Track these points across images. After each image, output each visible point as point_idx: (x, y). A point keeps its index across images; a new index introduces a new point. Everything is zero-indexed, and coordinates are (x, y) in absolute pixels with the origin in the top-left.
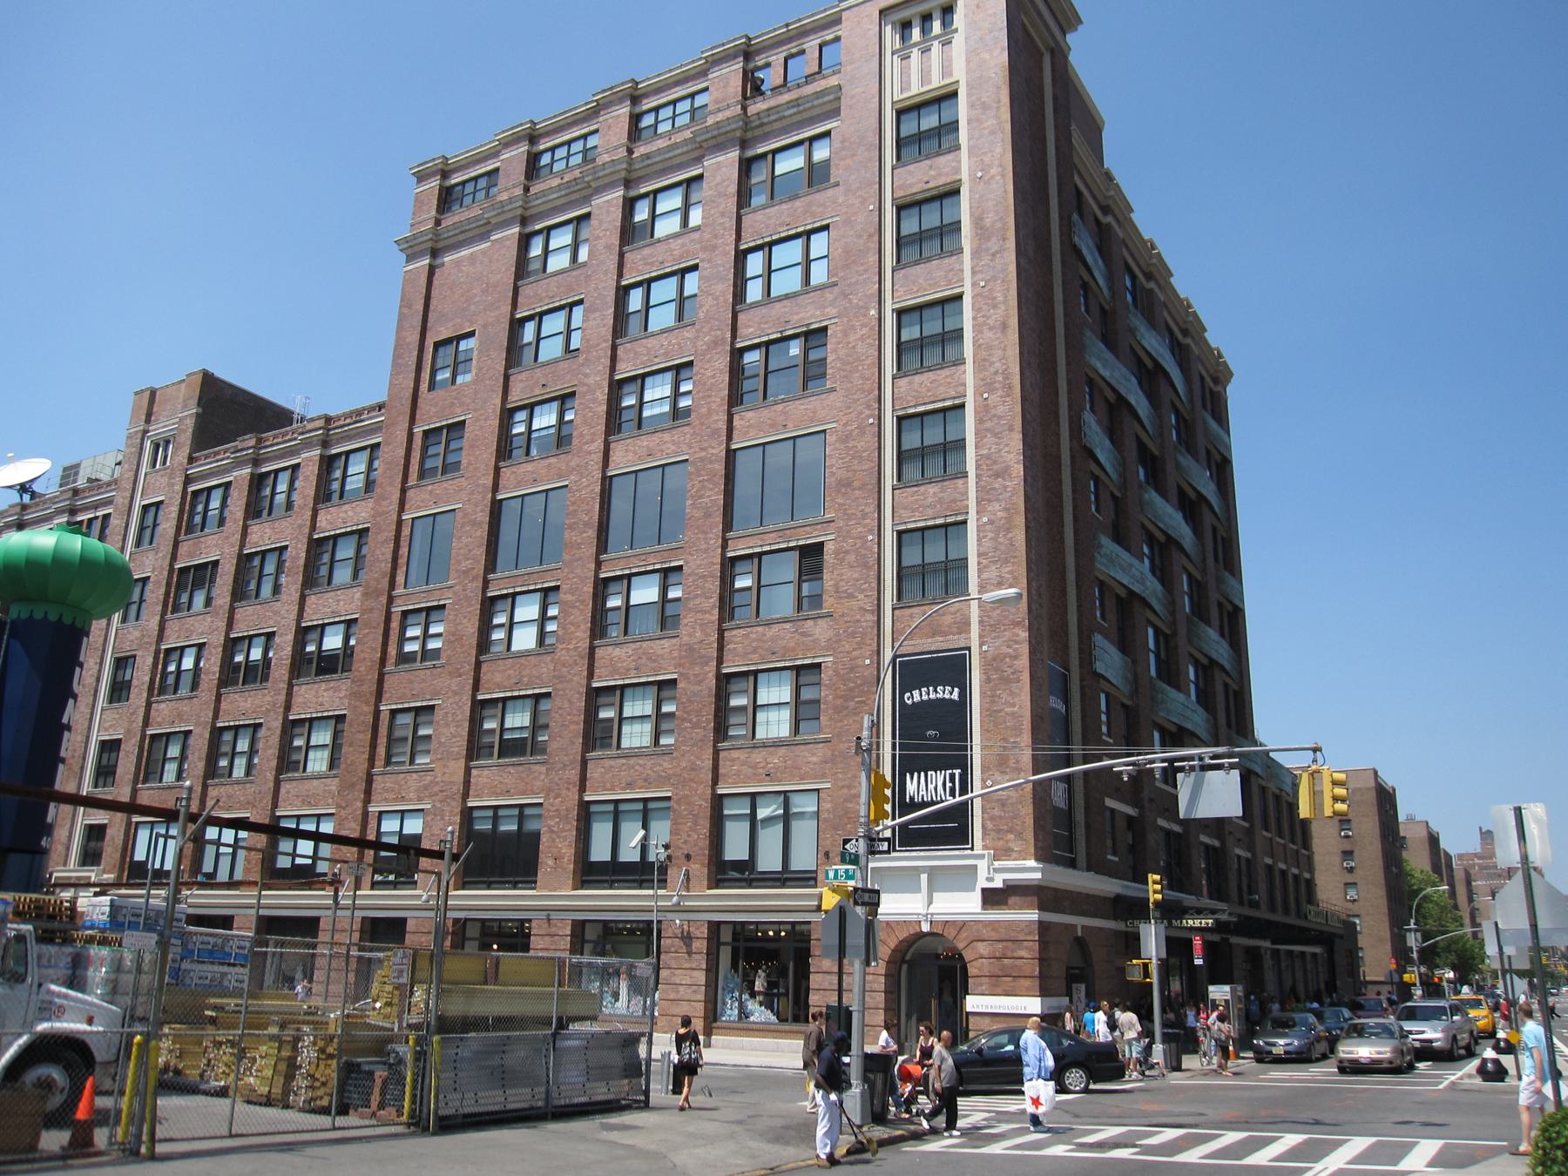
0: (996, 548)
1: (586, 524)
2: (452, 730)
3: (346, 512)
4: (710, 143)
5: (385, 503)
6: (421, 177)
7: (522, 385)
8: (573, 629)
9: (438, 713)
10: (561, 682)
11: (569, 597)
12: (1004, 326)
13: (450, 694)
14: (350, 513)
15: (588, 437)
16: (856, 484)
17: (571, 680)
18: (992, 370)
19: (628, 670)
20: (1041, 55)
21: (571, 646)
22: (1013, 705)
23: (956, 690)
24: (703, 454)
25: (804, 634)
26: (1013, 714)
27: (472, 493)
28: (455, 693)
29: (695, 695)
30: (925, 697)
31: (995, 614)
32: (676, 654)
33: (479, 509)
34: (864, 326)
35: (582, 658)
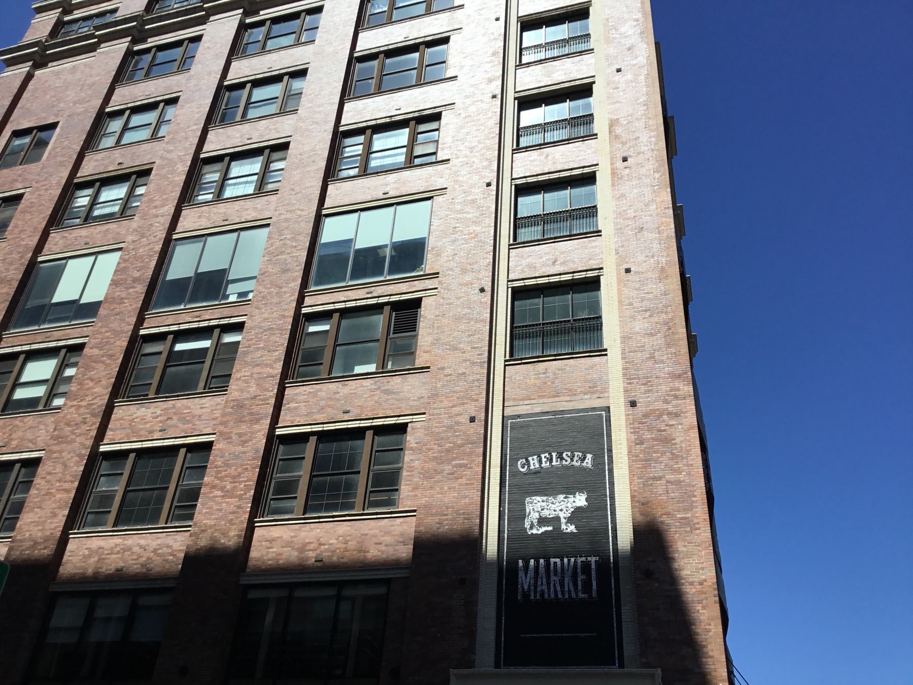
1: (135, 280)
7: (95, 164)
8: (91, 384)
10: (59, 443)
11: (96, 351)
15: (157, 203)
17: (73, 441)
22: (679, 471)
23: (589, 456)
25: (387, 392)
26: (678, 482)
27: (11, 253)
29: (237, 457)
32: (217, 414)
33: (12, 268)
35: (94, 415)
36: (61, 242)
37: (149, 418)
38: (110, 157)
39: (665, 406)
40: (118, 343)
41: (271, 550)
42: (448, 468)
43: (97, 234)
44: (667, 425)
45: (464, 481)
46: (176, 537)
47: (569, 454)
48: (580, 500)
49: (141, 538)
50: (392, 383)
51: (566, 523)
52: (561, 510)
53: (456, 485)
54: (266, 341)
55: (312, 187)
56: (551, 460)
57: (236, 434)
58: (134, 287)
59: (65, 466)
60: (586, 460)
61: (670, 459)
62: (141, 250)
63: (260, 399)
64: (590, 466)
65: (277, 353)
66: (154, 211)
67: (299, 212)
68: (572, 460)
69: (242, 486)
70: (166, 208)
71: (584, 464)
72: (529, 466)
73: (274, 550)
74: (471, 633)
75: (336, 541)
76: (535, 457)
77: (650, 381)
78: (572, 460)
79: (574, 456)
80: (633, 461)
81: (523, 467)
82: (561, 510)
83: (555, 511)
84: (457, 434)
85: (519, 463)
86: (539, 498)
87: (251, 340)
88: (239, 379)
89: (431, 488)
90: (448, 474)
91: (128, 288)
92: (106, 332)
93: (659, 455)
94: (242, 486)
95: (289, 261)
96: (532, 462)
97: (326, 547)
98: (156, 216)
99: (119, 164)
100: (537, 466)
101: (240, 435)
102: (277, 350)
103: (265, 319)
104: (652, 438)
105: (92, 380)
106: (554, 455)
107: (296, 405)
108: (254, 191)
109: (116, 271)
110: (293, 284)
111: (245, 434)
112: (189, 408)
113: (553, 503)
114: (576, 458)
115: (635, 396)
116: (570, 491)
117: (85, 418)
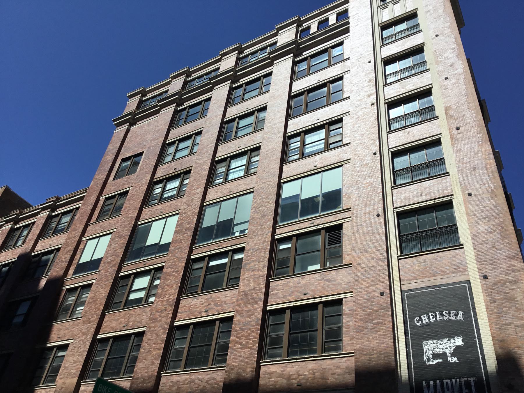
1: (187, 229)
2: (75, 358)
3: (53, 241)
5: (75, 232)
7: (163, 170)
8: (168, 288)
9: (70, 348)
10: (153, 322)
11: (169, 270)
13: (81, 335)
14: (55, 241)
15: (195, 187)
17: (161, 321)
19: (200, 313)
21: (165, 299)
23: (461, 313)
27: (124, 222)
28: (84, 334)
29: (247, 324)
32: (235, 300)
33: (125, 229)
35: (170, 305)
36: (148, 213)
37: (199, 305)
38: (170, 166)
39: (507, 277)
40: (180, 264)
41: (271, 379)
42: (371, 325)
43: (166, 207)
44: (510, 289)
45: (381, 333)
46: (218, 373)
47: (447, 312)
48: (459, 341)
49: (199, 375)
50: (330, 275)
51: (451, 357)
52: (447, 348)
54: (257, 256)
55: (275, 168)
56: (436, 317)
57: (245, 311)
58: (186, 233)
59: (157, 335)
60: (459, 316)
61: (515, 311)
62: (189, 213)
63: (257, 290)
64: (462, 319)
65: (264, 263)
66: (194, 191)
67: (268, 183)
68: (450, 316)
69: (251, 341)
70: (200, 189)
71: (458, 318)
72: (422, 321)
73: (273, 379)
75: (308, 373)
76: (425, 315)
77: (494, 262)
78: (450, 316)
79: (450, 313)
80: (491, 314)
81: (418, 322)
82: (447, 348)
83: (442, 349)
84: (374, 303)
85: (415, 319)
86: (431, 342)
87: (249, 256)
88: (244, 279)
89: (362, 338)
90: (371, 329)
91: (183, 234)
92: (174, 259)
93: (507, 309)
94: (251, 341)
95: (265, 210)
96: (423, 319)
97: (303, 377)
98: (195, 194)
99: (175, 169)
100: (427, 321)
101: (248, 311)
102: (263, 261)
103: (256, 244)
104: (501, 298)
105: (168, 286)
106: (437, 313)
107: (277, 292)
108: (244, 174)
109: (177, 226)
110: (269, 223)
111: (250, 311)
112: (219, 297)
113: (440, 344)
114: (452, 315)
115: (486, 272)
116: (451, 336)
117: (166, 307)
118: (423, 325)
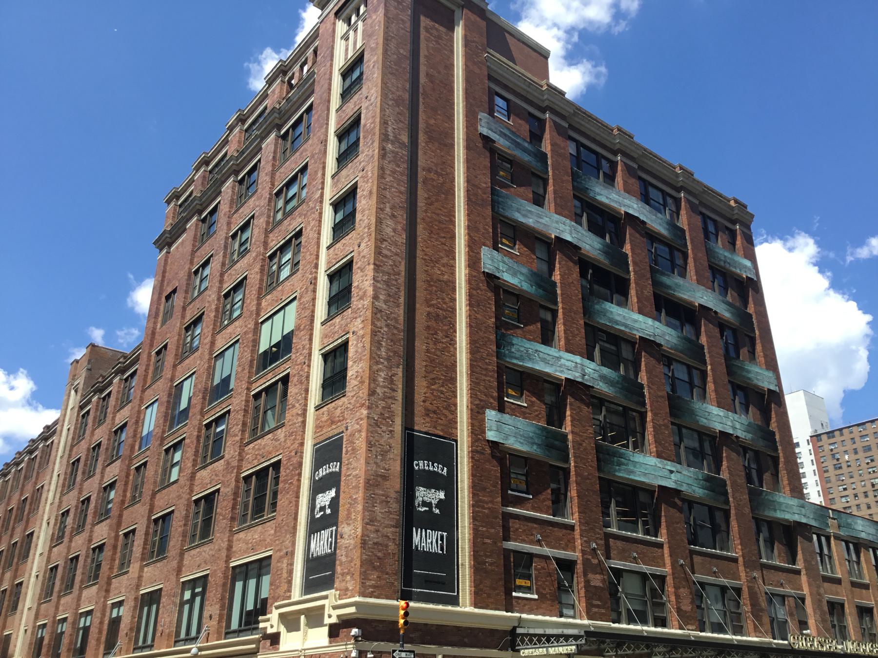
0: (356, 352)
4: (265, 133)
6: (168, 202)
12: (371, 193)
16: (302, 327)
18: (363, 225)
20: (453, 11)
24: (246, 329)
30: (324, 473)
31: (352, 401)
34: (313, 220)
48: (332, 493)
53: (288, 496)
74: (290, 582)
101: (228, 481)
105: (187, 458)
118: (320, 479)
